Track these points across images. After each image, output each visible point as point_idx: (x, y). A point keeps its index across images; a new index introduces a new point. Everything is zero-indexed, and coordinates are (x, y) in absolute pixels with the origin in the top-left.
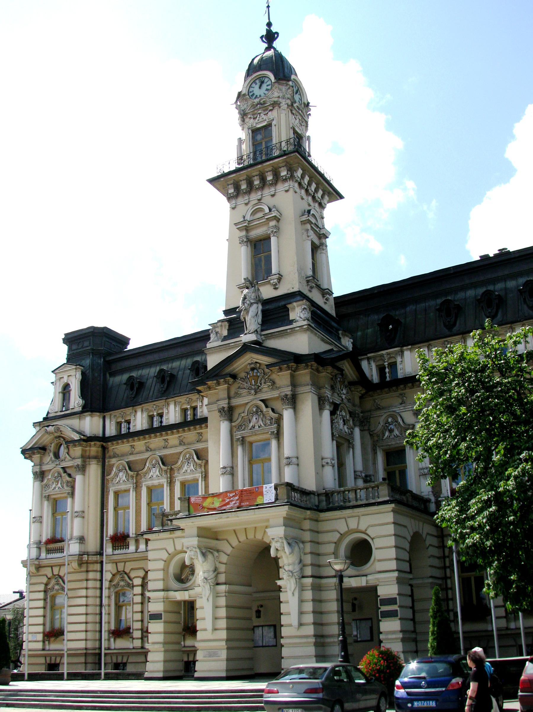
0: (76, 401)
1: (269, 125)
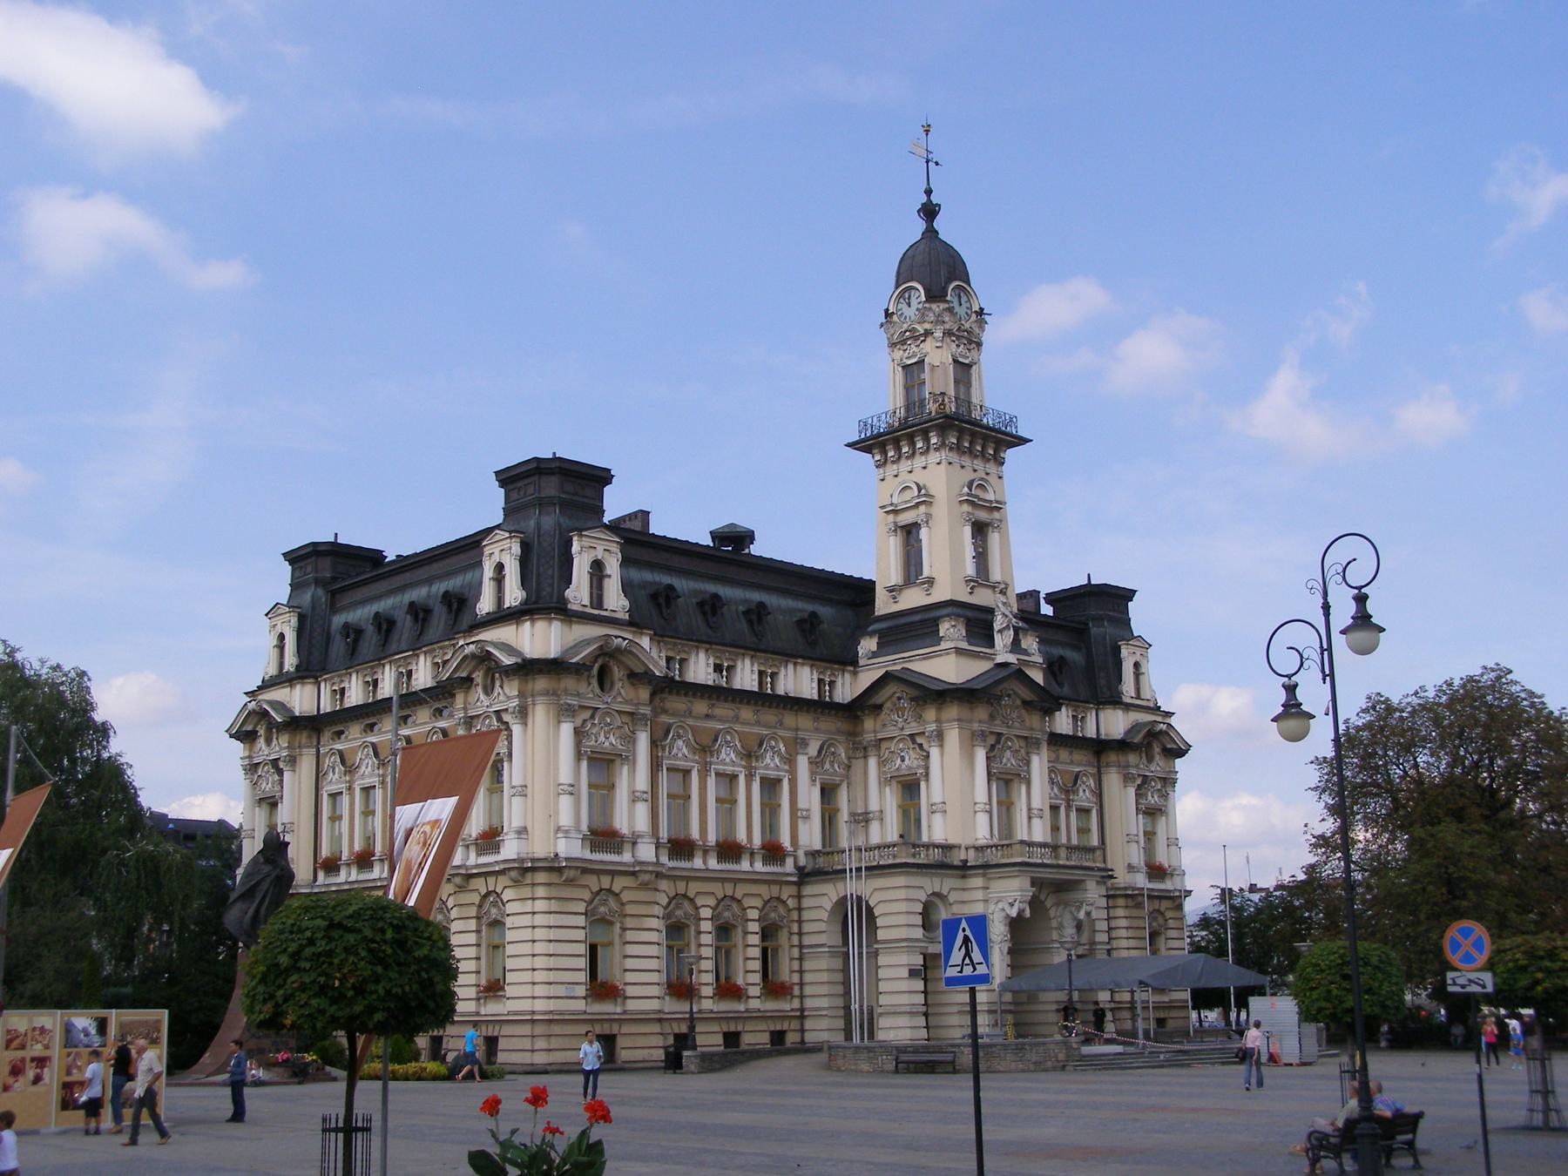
0: (616, 601)
1: (969, 366)
